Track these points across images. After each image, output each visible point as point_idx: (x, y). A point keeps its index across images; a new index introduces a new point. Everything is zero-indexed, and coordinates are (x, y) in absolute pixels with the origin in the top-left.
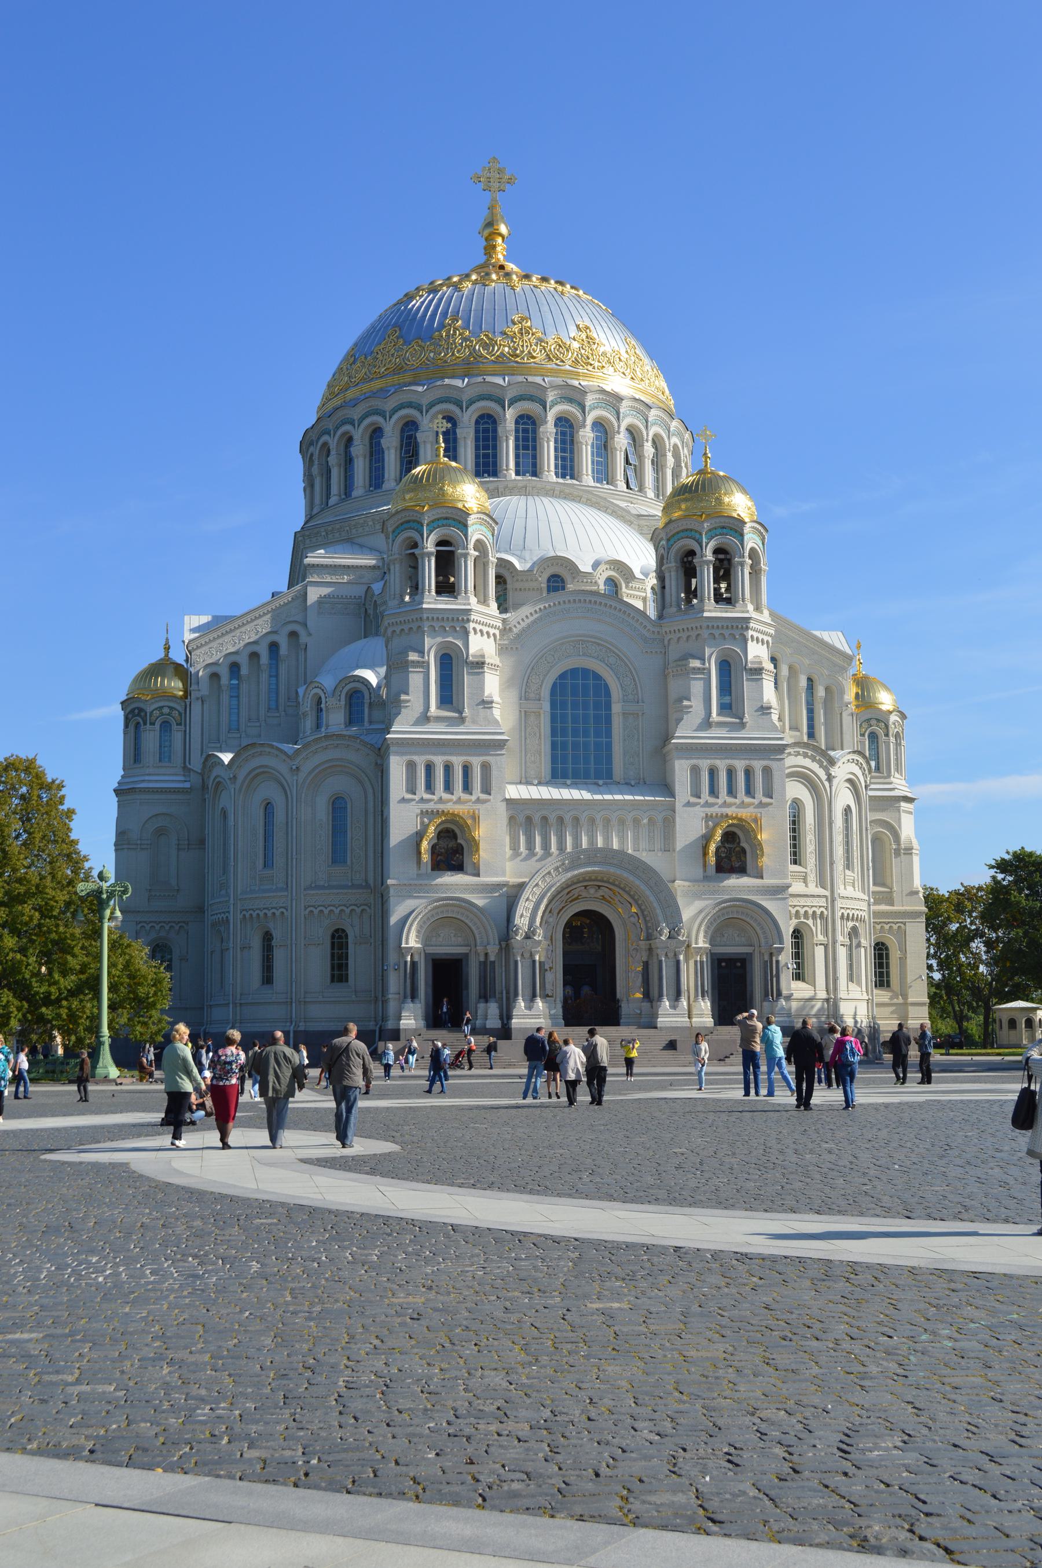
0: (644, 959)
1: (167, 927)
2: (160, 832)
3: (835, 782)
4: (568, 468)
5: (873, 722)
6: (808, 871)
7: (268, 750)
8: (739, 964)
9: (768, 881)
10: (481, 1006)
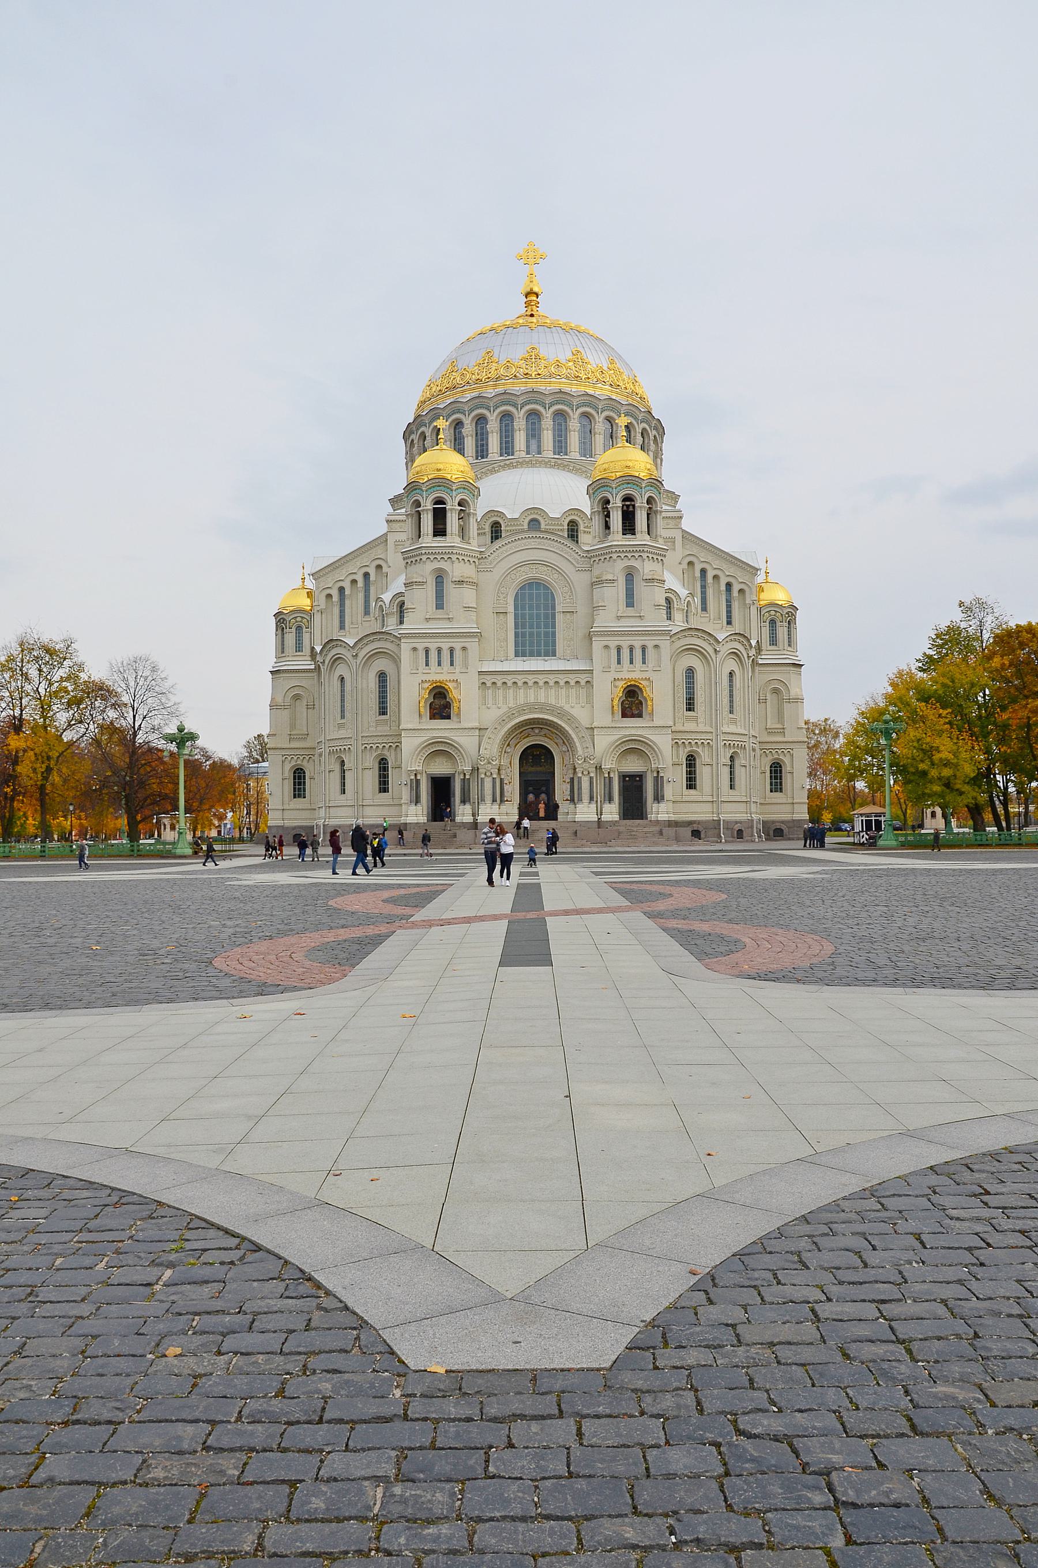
2: (297, 697)
3: (719, 656)
4: (561, 446)
5: (773, 613)
6: (699, 715)
9: (657, 722)
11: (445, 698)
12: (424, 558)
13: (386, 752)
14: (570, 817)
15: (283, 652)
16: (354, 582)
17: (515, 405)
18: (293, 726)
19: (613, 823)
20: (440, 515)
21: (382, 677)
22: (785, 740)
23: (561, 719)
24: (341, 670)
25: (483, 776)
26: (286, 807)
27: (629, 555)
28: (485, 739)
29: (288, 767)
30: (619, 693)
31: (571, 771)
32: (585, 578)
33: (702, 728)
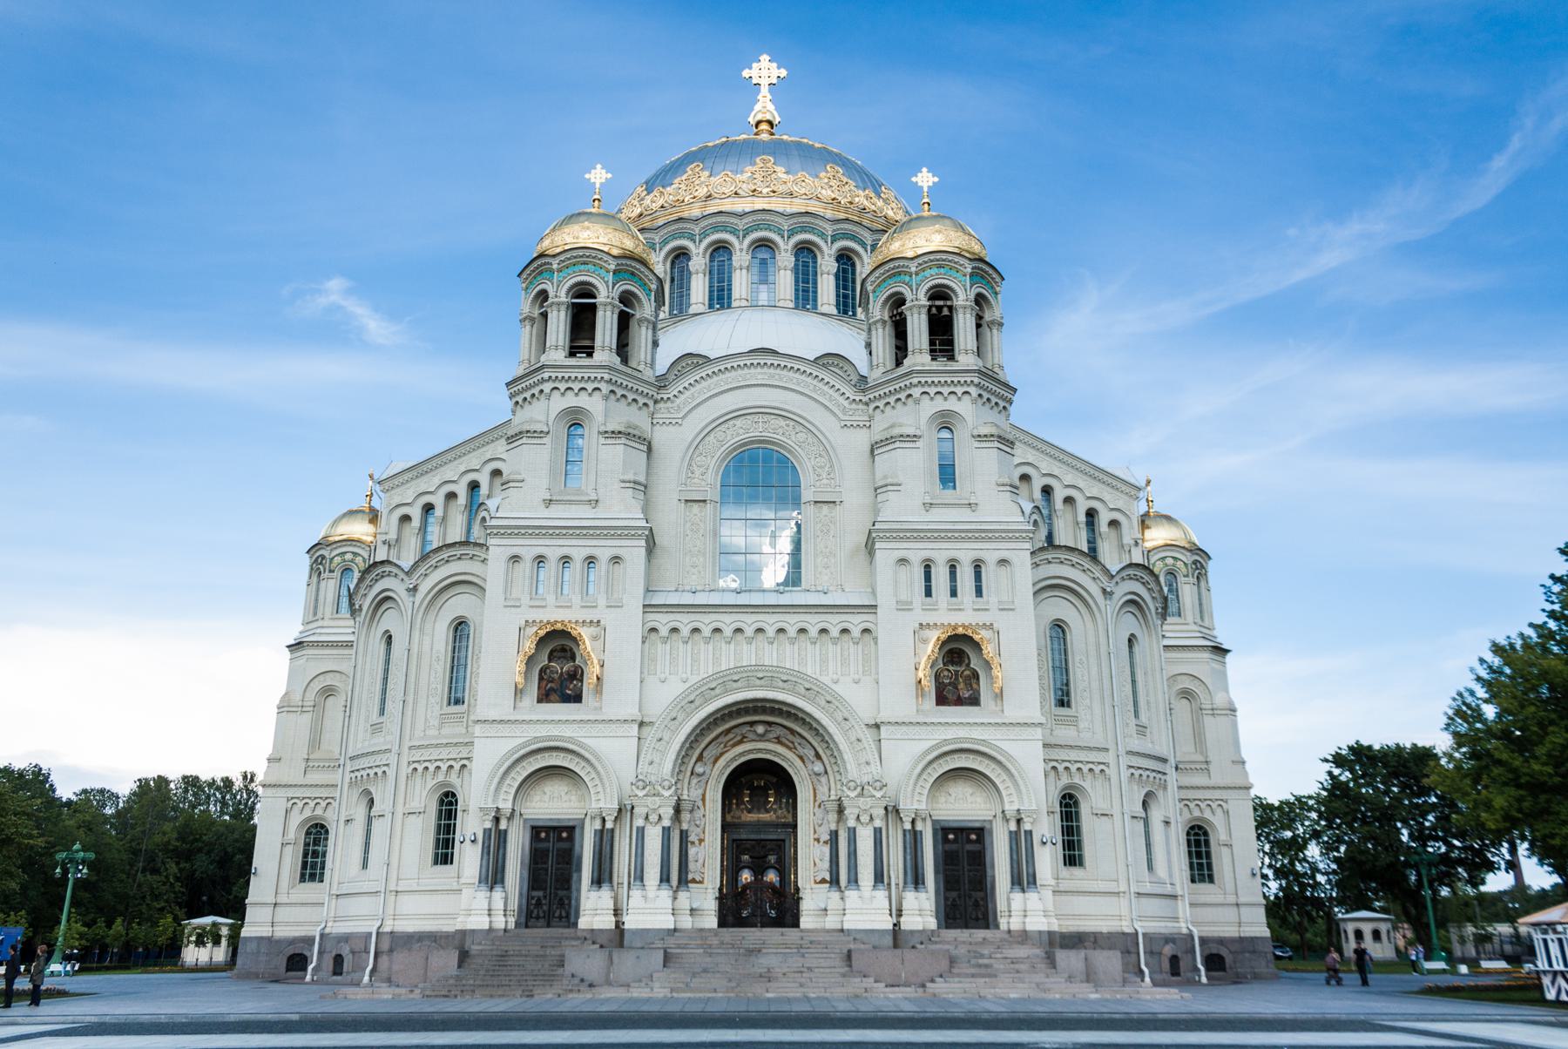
0: (833, 827)
1: (323, 804)
7: (387, 568)
8: (973, 837)
9: (1012, 713)
10: (594, 894)
11: (573, 658)
12: (547, 387)
13: (453, 778)
14: (831, 922)
15: (315, 614)
16: (451, 496)
17: (734, 232)
18: (315, 742)
19: (926, 937)
20: (582, 318)
21: (460, 627)
22: (1211, 783)
23: (812, 701)
24: (389, 620)
25: (639, 822)
26: (282, 899)
27: (946, 390)
28: (646, 744)
29: (296, 819)
30: (930, 648)
31: (833, 817)
32: (862, 439)
33: (1086, 739)
